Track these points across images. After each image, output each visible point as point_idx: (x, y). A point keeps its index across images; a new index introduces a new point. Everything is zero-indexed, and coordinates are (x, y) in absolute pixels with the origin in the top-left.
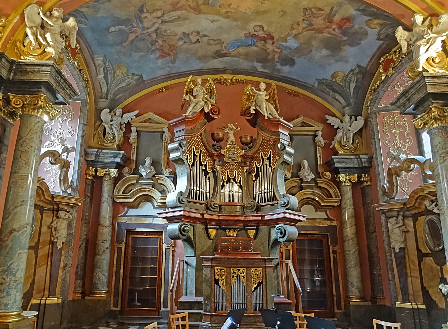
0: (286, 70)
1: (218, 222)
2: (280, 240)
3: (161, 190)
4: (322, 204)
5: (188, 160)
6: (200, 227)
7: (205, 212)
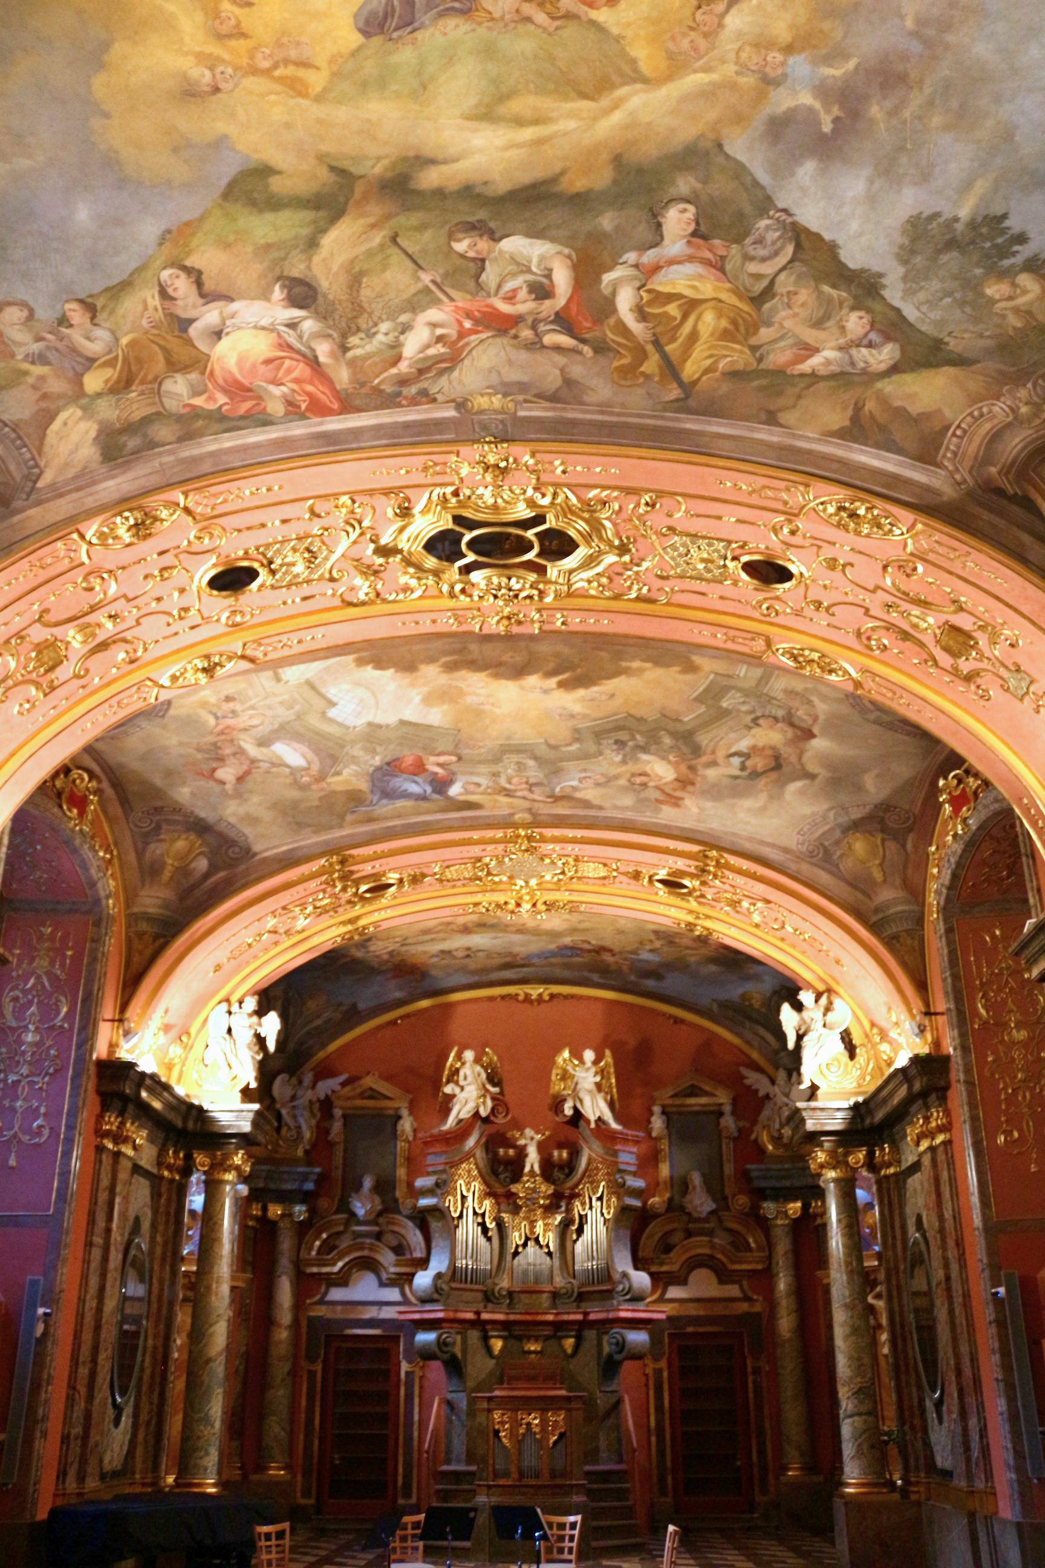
0: (650, 984)
1: (505, 1325)
2: (618, 1357)
6: (474, 1335)
7: (481, 1306)
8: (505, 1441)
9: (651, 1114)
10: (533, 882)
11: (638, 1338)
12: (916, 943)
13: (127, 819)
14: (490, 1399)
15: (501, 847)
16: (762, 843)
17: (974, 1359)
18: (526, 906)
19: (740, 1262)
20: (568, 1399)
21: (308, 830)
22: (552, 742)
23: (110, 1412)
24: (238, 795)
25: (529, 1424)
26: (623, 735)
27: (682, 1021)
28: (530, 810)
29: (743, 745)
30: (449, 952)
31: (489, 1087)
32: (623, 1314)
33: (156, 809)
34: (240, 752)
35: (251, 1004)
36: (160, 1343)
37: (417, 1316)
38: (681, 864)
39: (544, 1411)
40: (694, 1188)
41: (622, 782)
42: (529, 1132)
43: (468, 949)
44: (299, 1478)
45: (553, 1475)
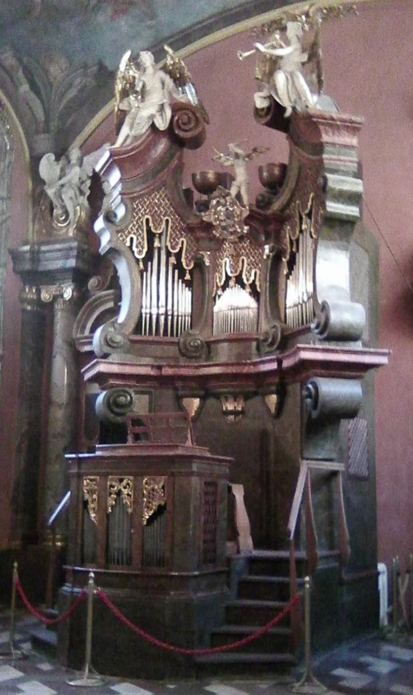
5: (134, 248)
8: (93, 515)
25: (119, 493)
39: (138, 475)
45: (146, 561)
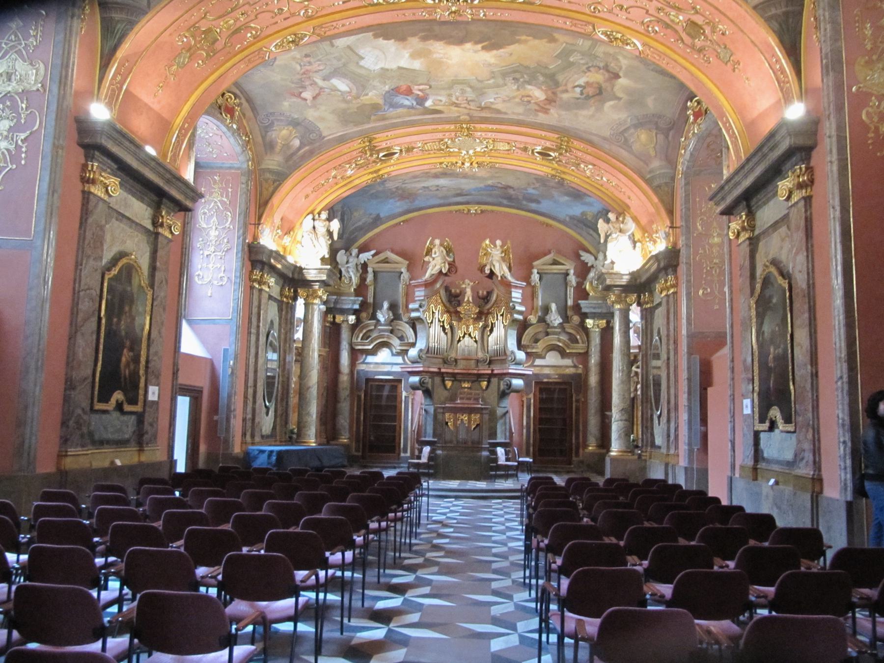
0: (533, 206)
2: (507, 391)
3: (400, 335)
4: (568, 351)
6: (438, 380)
7: (441, 366)
9: (531, 273)
10: (471, 152)
11: (518, 383)
12: (670, 190)
13: (256, 118)
14: (443, 408)
15: (453, 134)
16: (591, 134)
17: (676, 396)
18: (467, 165)
19: (573, 349)
20: (482, 409)
21: (352, 124)
22: (479, 78)
23: (264, 410)
24: (314, 106)
25: (462, 420)
26: (518, 75)
27: (551, 226)
28: (468, 114)
29: (582, 81)
30: (428, 188)
31: (447, 258)
32: (510, 371)
33: (271, 113)
34: (314, 84)
35: (324, 215)
36: (285, 379)
37: (410, 370)
38: (548, 144)
40: (552, 312)
41: (517, 100)
42: (467, 281)
43: (438, 186)
44: (354, 444)
